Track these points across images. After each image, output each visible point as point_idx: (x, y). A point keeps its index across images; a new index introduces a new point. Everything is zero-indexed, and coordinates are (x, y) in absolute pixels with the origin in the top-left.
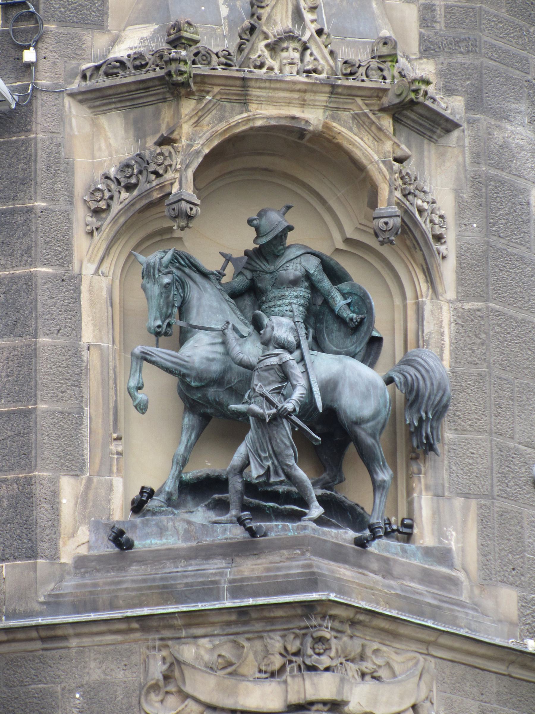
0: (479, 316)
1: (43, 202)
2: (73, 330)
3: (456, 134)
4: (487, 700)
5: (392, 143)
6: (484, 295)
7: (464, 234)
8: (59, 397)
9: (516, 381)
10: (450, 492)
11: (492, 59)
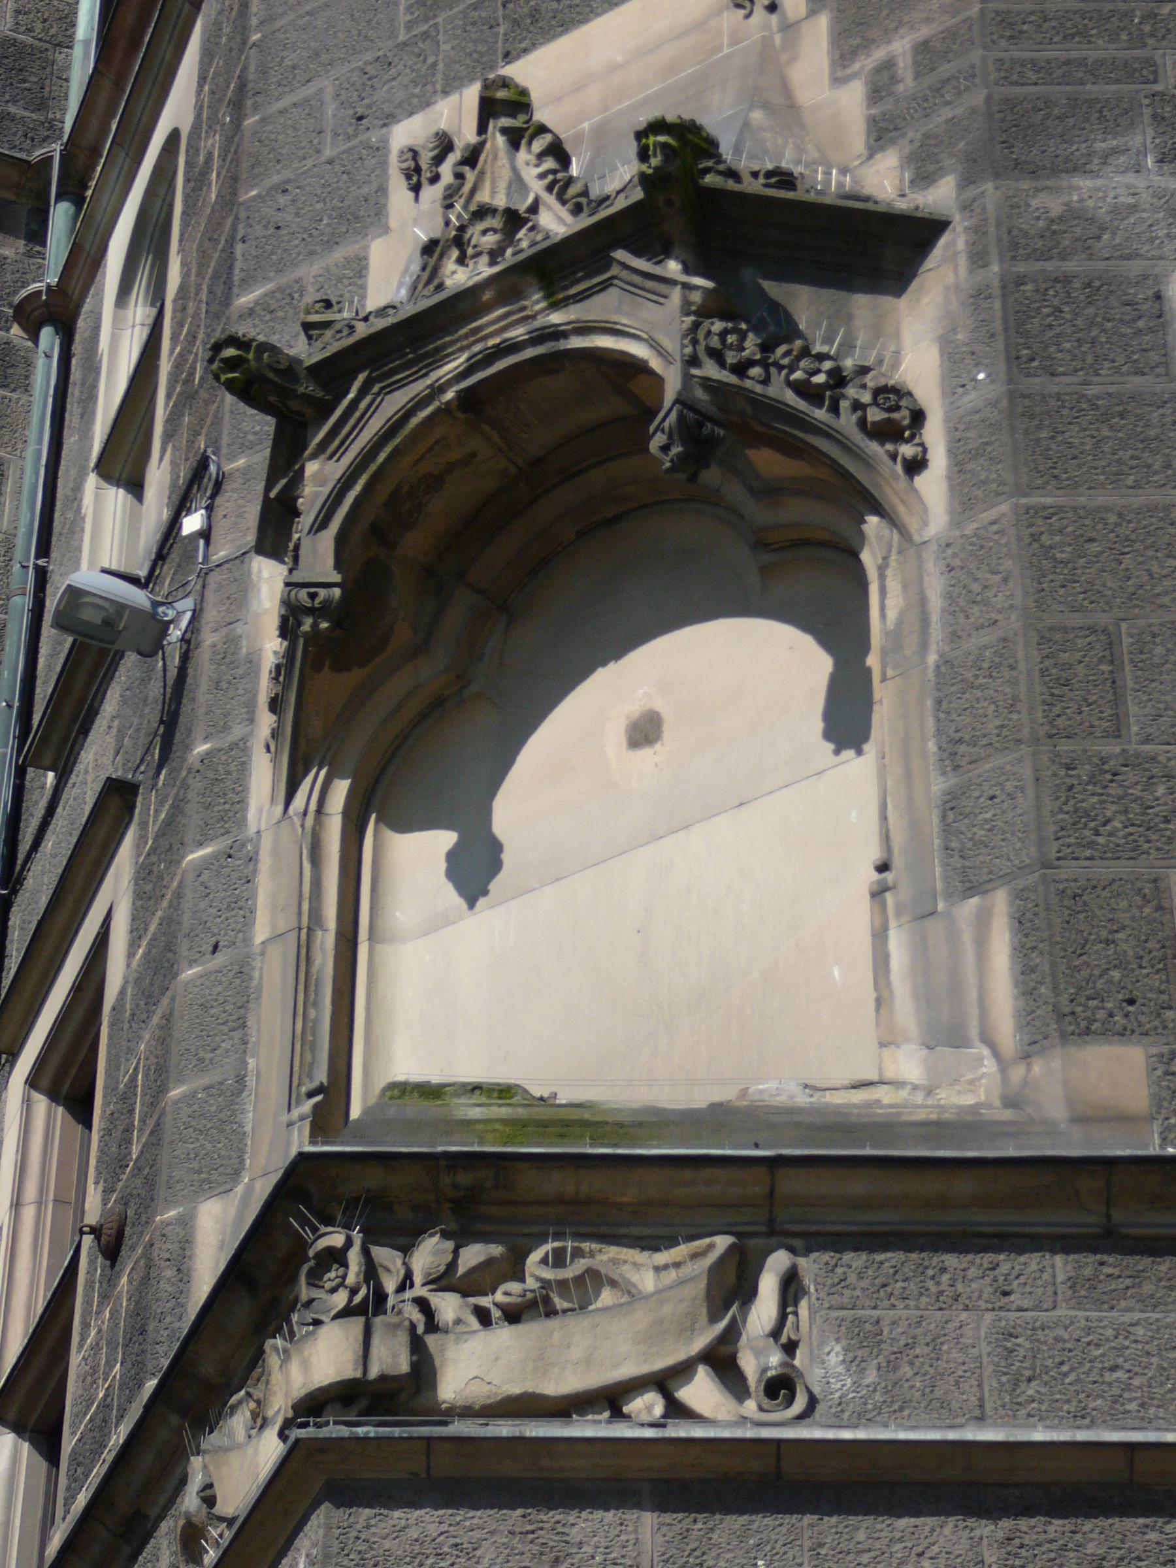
0: (996, 533)
1: (205, 743)
2: (240, 931)
3: (943, 241)
4: (1026, 1303)
5: (679, 287)
6: (1006, 489)
7: (959, 403)
8: (207, 1062)
9: (1124, 625)
10: (949, 896)
11: (1023, 85)
